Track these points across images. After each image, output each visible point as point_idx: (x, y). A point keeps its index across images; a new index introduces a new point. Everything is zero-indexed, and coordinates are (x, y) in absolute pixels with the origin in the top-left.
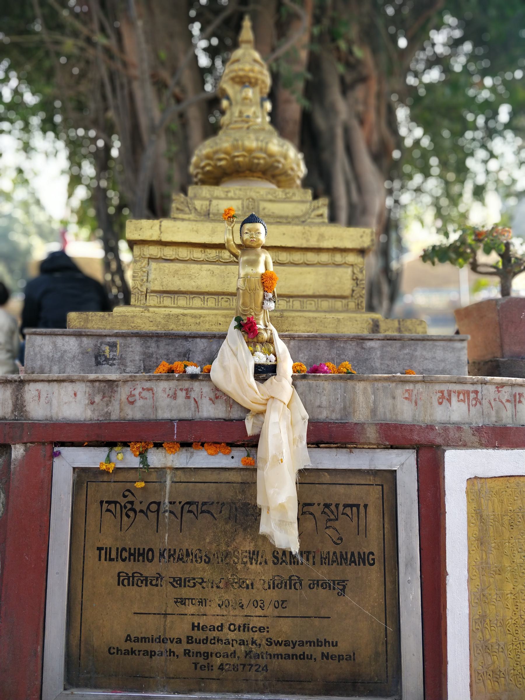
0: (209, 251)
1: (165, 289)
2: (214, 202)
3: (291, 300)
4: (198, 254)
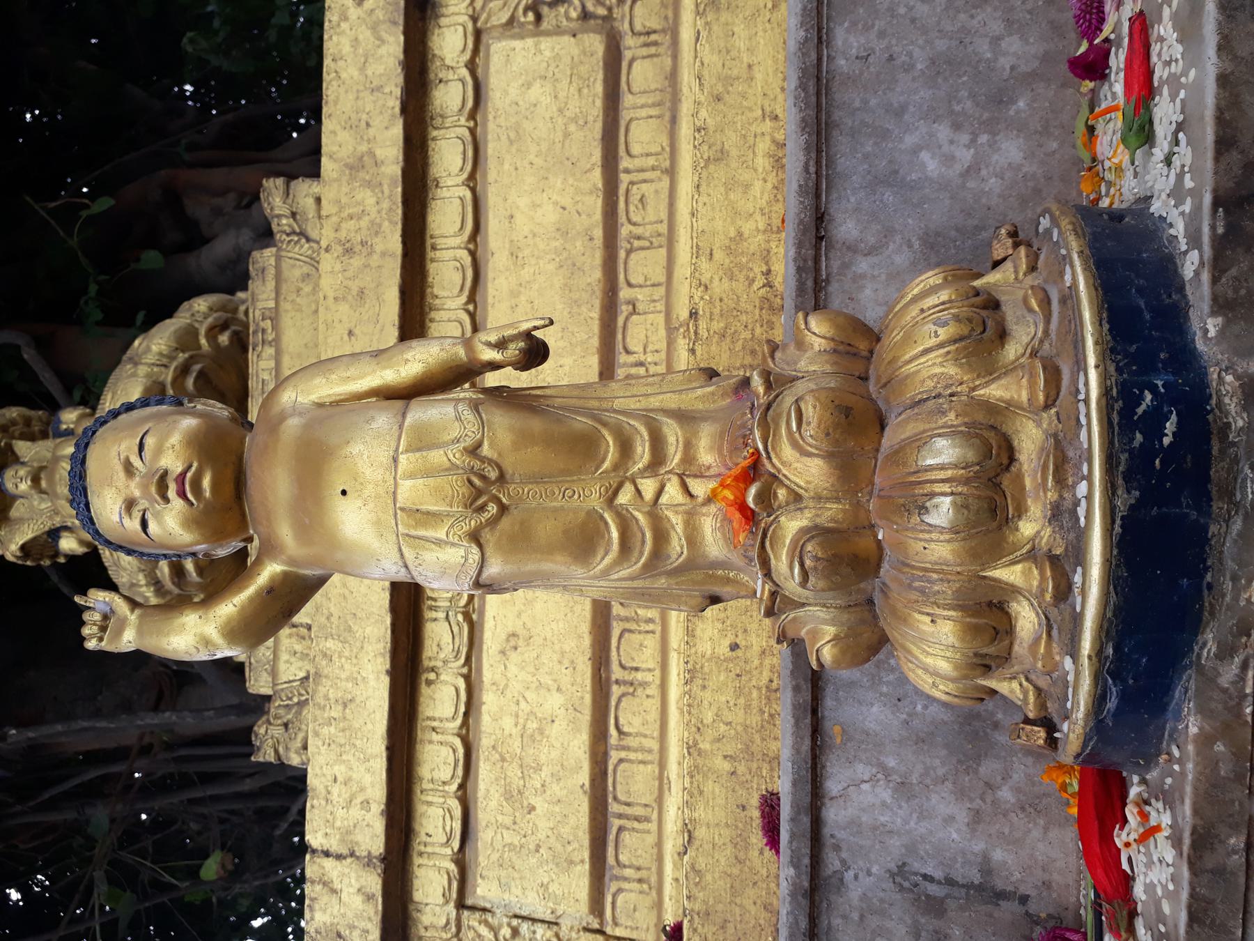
1: (586, 855)
3: (624, 293)
4: (440, 701)
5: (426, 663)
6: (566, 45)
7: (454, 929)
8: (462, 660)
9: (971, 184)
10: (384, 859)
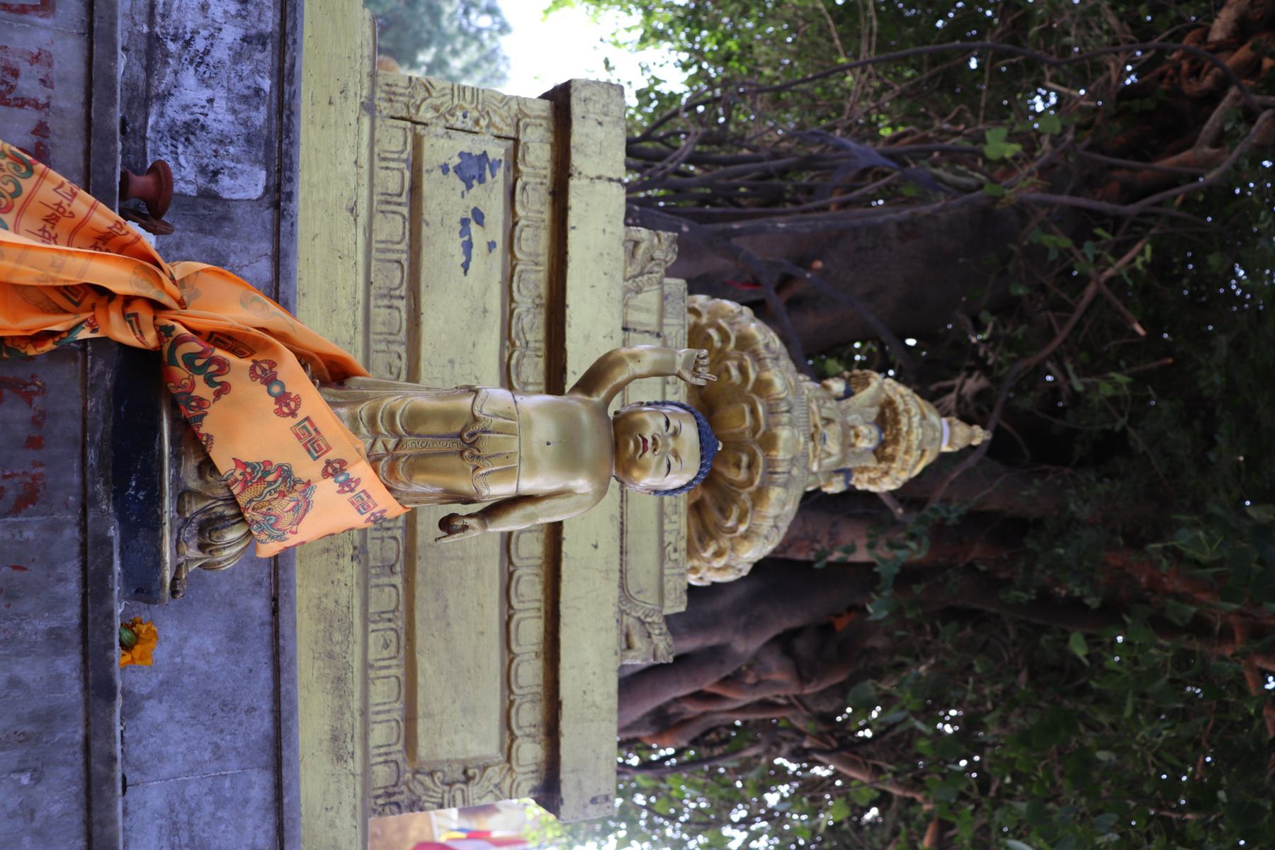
3: (398, 580)
5: (543, 311)
6: (443, 754)
7: (521, 124)
8: (516, 312)
9: (185, 632)
10: (570, 175)
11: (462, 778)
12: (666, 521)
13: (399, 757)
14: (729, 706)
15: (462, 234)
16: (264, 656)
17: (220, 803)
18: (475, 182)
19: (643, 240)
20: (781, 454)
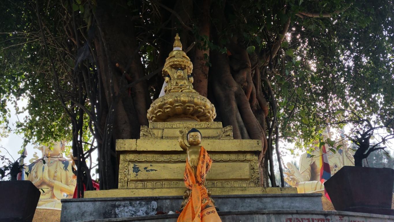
0: (165, 156)
2: (166, 130)
3: (215, 182)
5: (163, 155)
6: (248, 173)
11: (253, 170)
12: (202, 127)
13: (249, 182)
14: (255, 90)
15: (149, 171)
16: (228, 200)
17: (250, 206)
18: (139, 169)
19: (143, 133)
20: (187, 99)
